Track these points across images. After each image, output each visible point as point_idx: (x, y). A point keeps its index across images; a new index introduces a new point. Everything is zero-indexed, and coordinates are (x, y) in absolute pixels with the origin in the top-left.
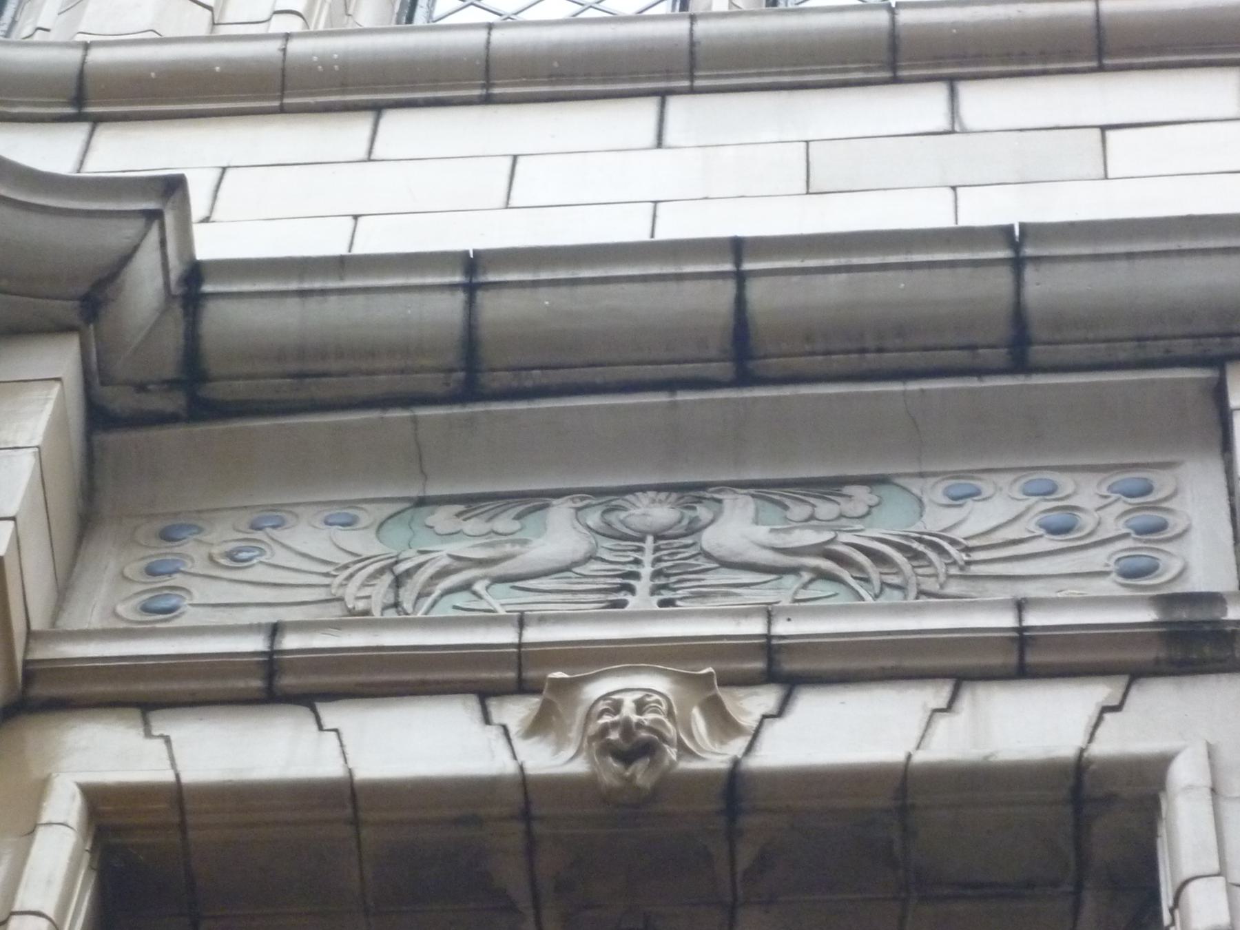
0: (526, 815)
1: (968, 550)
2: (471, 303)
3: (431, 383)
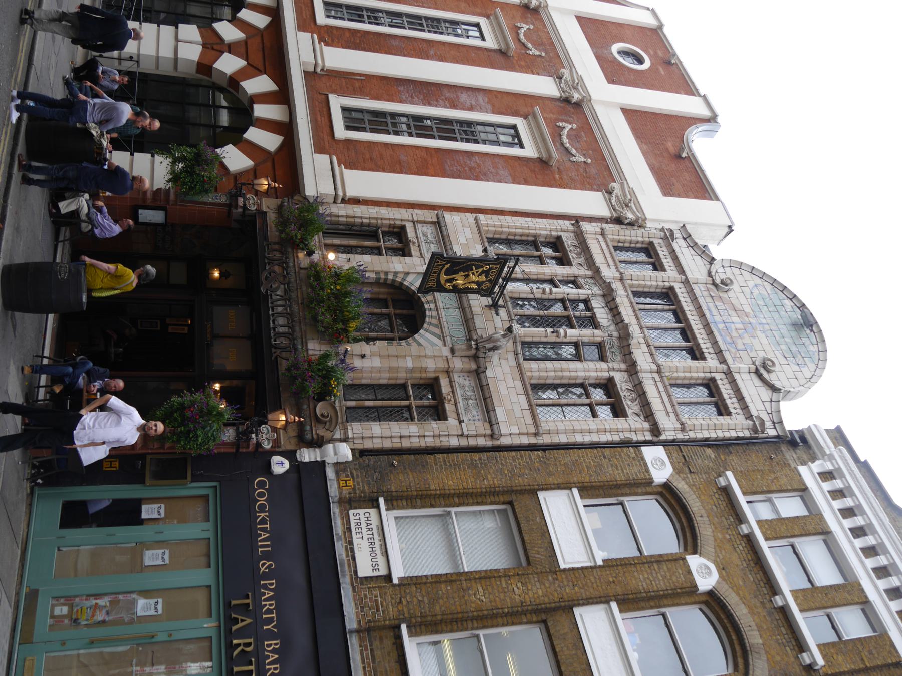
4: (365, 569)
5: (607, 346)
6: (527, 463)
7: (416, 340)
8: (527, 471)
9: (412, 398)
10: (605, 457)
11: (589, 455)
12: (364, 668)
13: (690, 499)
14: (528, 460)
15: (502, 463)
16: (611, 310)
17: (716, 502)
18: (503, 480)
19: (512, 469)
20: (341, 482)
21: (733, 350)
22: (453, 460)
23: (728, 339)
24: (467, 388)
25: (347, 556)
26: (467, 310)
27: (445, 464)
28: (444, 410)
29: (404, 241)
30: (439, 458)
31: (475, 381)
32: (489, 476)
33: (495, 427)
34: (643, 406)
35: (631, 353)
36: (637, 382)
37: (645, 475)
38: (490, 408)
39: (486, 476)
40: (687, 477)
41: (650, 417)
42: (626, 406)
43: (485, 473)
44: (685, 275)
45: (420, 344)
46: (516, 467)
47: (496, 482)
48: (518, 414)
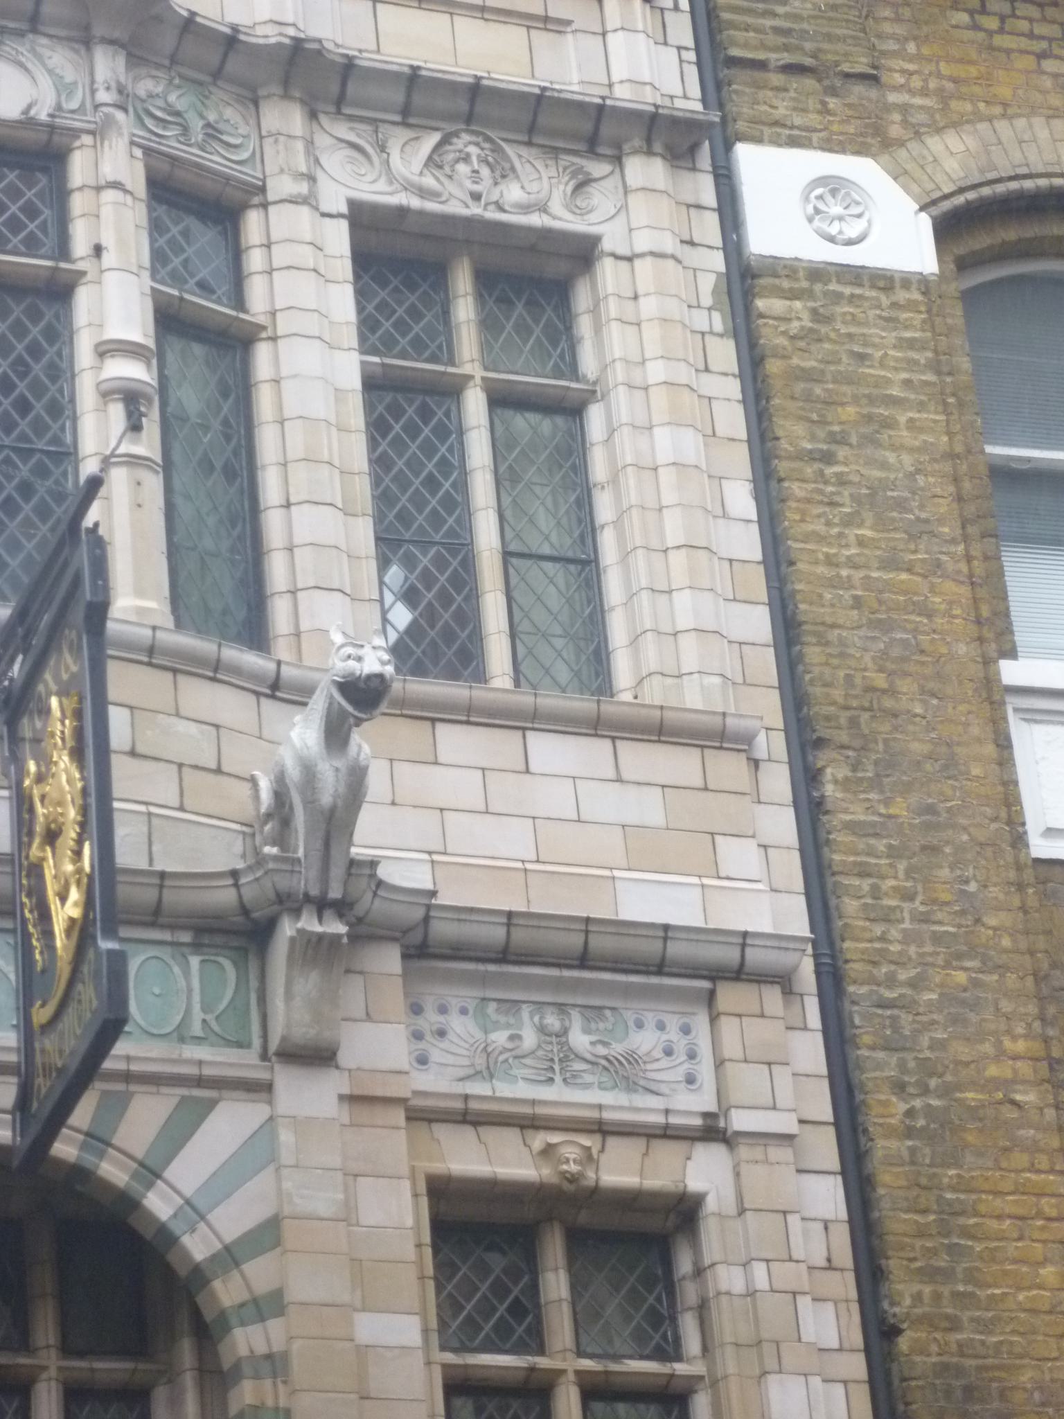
0: (539, 1189)
1: (645, 1063)
2: (508, 932)
3: (493, 955)
5: (172, 144)
6: (893, 853)
7: (231, 1257)
8: (945, 873)
9: (543, 1362)
10: (828, 458)
11: (819, 527)
13: (1017, 156)
14: (881, 845)
15: (913, 984)
17: (1024, 43)
18: (1006, 1006)
19: (937, 938)
22: (921, 1233)
24: (500, 1038)
27: (947, 1275)
28: (629, 1200)
30: (918, 1298)
31: (450, 978)
32: (992, 1071)
33: (755, 957)
34: (532, 129)
35: (231, 41)
36: (399, 97)
37: (910, 306)
38: (651, 948)
39: (997, 1083)
40: (904, 109)
41: (606, 130)
42: (535, 220)
43: (973, 1085)
46: (925, 919)
47: (1021, 1046)
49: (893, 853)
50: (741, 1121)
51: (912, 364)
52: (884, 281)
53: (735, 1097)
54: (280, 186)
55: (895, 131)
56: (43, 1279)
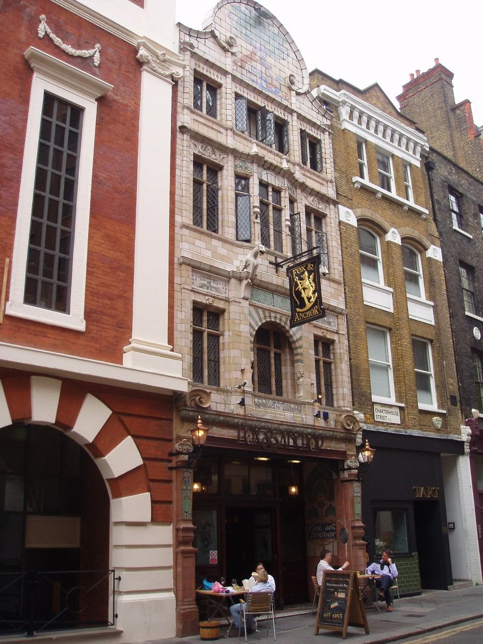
4: (395, 419)
7: (298, 340)
12: (428, 431)
15: (354, 317)
16: (268, 169)
20: (368, 422)
21: (280, 94)
23: (273, 89)
25: (392, 427)
26: (279, 289)
28: (329, 339)
29: (201, 307)
38: (333, 309)
41: (329, 201)
44: (229, 73)
45: (301, 338)
48: (332, 291)
49: (352, 301)
50: (341, 332)
51: (355, 238)
52: (352, 226)
53: (340, 329)
54: (299, 201)
55: (354, 207)
56: (272, 338)
